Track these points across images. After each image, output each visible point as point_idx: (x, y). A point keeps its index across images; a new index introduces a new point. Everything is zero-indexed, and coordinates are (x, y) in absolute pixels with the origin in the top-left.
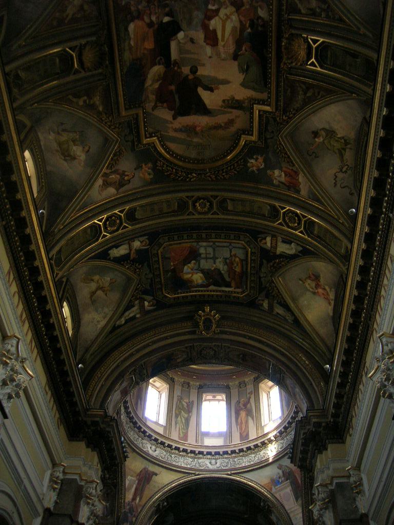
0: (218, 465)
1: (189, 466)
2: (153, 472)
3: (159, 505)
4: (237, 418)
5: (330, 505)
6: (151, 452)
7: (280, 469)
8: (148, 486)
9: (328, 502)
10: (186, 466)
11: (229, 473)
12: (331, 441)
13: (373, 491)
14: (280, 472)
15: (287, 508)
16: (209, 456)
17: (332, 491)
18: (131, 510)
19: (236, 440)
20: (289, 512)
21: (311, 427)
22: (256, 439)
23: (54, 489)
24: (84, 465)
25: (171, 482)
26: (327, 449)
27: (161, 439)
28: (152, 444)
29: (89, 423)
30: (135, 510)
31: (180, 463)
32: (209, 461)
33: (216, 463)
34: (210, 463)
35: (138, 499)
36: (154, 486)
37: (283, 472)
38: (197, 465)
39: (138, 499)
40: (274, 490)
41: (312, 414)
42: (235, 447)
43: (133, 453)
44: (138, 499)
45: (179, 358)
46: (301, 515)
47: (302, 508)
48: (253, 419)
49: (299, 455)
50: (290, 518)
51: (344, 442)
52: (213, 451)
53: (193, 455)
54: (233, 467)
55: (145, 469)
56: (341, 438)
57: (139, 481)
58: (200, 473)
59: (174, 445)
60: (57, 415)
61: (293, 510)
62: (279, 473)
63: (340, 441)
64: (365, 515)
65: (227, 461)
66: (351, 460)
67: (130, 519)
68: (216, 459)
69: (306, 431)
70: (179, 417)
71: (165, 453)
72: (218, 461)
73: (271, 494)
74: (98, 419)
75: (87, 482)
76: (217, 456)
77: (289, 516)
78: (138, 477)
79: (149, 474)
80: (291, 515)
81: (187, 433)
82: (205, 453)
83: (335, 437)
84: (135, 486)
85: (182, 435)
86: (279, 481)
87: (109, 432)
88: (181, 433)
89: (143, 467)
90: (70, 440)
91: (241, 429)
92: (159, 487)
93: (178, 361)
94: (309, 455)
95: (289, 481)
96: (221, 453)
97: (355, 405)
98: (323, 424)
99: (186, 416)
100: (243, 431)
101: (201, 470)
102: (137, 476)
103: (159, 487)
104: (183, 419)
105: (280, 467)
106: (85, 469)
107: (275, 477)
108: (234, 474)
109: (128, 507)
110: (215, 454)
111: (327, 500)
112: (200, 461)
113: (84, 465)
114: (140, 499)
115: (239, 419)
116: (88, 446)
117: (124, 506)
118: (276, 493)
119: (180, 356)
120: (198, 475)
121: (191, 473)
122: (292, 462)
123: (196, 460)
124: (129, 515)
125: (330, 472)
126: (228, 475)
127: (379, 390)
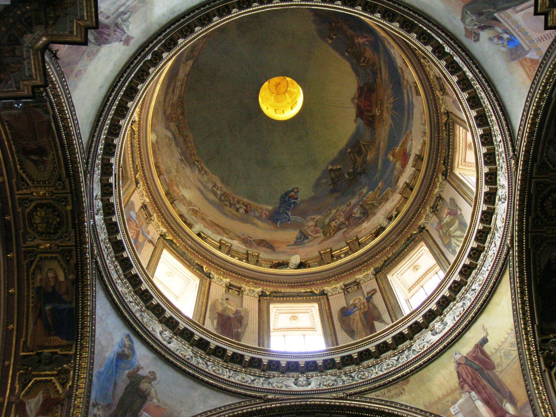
2: (477, 346)
7: (478, 35)
8: (497, 370)
14: (484, 35)
36: (507, 355)
37: (482, 28)
43: (408, 382)
45: (56, 278)
55: (459, 364)
57: (474, 388)
62: (491, 39)
78: (466, 387)
79: (476, 358)
84: (479, 404)
89: (452, 367)
92: (512, 345)
93: (62, 278)
95: (496, 15)
102: (462, 387)
107: (504, 49)
114: (513, 401)
118: (538, 50)
119: (51, 275)
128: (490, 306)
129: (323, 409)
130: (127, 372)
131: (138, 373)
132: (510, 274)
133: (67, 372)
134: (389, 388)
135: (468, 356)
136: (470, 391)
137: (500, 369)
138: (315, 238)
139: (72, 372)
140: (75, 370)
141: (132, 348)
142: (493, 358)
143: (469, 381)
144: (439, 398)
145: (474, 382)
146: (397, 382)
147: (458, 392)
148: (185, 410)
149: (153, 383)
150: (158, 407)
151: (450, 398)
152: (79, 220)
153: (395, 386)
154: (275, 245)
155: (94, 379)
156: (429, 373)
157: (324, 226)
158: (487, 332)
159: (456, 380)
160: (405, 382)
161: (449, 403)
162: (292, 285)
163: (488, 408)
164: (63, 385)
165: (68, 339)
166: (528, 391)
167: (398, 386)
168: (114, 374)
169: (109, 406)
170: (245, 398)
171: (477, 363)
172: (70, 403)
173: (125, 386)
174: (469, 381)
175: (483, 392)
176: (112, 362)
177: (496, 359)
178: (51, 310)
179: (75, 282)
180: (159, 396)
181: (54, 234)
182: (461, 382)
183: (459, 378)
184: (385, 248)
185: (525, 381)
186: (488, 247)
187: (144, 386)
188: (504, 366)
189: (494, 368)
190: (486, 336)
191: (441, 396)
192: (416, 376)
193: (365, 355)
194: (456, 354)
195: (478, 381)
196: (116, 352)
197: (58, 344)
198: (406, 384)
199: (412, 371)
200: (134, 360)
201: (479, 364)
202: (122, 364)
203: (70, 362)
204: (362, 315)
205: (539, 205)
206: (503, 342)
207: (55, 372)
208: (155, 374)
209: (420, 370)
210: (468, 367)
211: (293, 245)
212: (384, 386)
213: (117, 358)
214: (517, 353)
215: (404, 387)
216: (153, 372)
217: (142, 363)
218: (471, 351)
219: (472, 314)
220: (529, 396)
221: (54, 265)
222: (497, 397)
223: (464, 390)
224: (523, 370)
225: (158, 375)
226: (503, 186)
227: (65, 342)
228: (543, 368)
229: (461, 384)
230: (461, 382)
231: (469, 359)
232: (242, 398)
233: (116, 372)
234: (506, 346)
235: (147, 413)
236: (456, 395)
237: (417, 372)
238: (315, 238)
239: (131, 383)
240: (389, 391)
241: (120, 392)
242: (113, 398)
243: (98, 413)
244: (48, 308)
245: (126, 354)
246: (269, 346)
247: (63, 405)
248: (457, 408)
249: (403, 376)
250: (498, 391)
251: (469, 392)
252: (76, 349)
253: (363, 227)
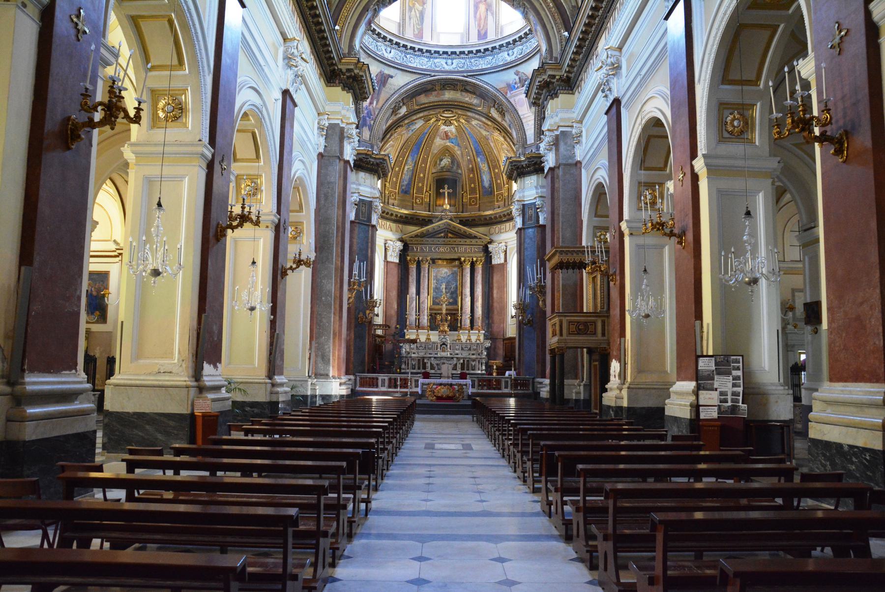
0: (454, 65)
1: (424, 67)
2: (389, 75)
3: (395, 106)
4: (475, 13)
5: (554, 148)
6: (386, 55)
7: (517, 75)
8: (384, 89)
9: (552, 145)
10: (421, 67)
11: (465, 74)
12: (562, 92)
13: (589, 145)
14: (517, 78)
15: (520, 113)
16: (445, 56)
17: (557, 136)
18: (369, 114)
19: (474, 39)
20: (521, 117)
21: (545, 77)
22: (495, 41)
23: (322, 136)
24: (343, 108)
25: (407, 84)
26: (558, 97)
27: (395, 40)
28: (386, 45)
29: (344, 70)
30: (373, 113)
31: (415, 64)
32: (445, 61)
33: (452, 63)
34: (446, 63)
36: (390, 88)
37: (520, 78)
38: (433, 65)
39: (375, 102)
40: (508, 95)
41: (549, 67)
42: (472, 47)
44: (375, 102)
46: (533, 122)
47: (535, 116)
48: (492, 14)
49: (533, 95)
50: (522, 124)
51: (573, 94)
52: (449, 50)
53: (428, 54)
54: (470, 69)
56: (572, 90)
58: (436, 74)
59: (409, 45)
60: (319, 71)
61: (525, 116)
62: (515, 79)
63: (571, 92)
64: (578, 164)
65: (463, 61)
66: (577, 112)
67: (368, 123)
68: (452, 59)
69: (541, 80)
70: (413, 10)
71: (400, 54)
72: (454, 61)
73: (506, 98)
74: (352, 67)
75: (347, 124)
76: (454, 56)
77: (521, 121)
80: (524, 121)
81: (422, 30)
82: (441, 53)
83: (567, 88)
85: (416, 32)
86: (514, 87)
87: (362, 76)
88: (416, 30)
89: (379, 71)
90: (327, 86)
91: (479, 25)
92: (394, 89)
94: (542, 97)
96: (458, 53)
97: (585, 72)
98: (557, 77)
99: (420, 8)
100: (481, 28)
101: (437, 71)
103: (394, 89)
104: (417, 12)
105: (517, 73)
106: (344, 112)
108: (470, 76)
109: (366, 112)
110: (450, 53)
111: (552, 143)
112: (436, 61)
113: (343, 108)
114: (377, 104)
115: (478, 14)
116: (343, 89)
117: (363, 111)
120: (434, 76)
121: (427, 75)
122: (526, 97)
123: (431, 60)
124: (367, 118)
125: (557, 119)
126: (464, 76)
127: (600, 85)
128: (405, 73)
142: (387, 84)
177: (388, 85)
192: (372, 60)
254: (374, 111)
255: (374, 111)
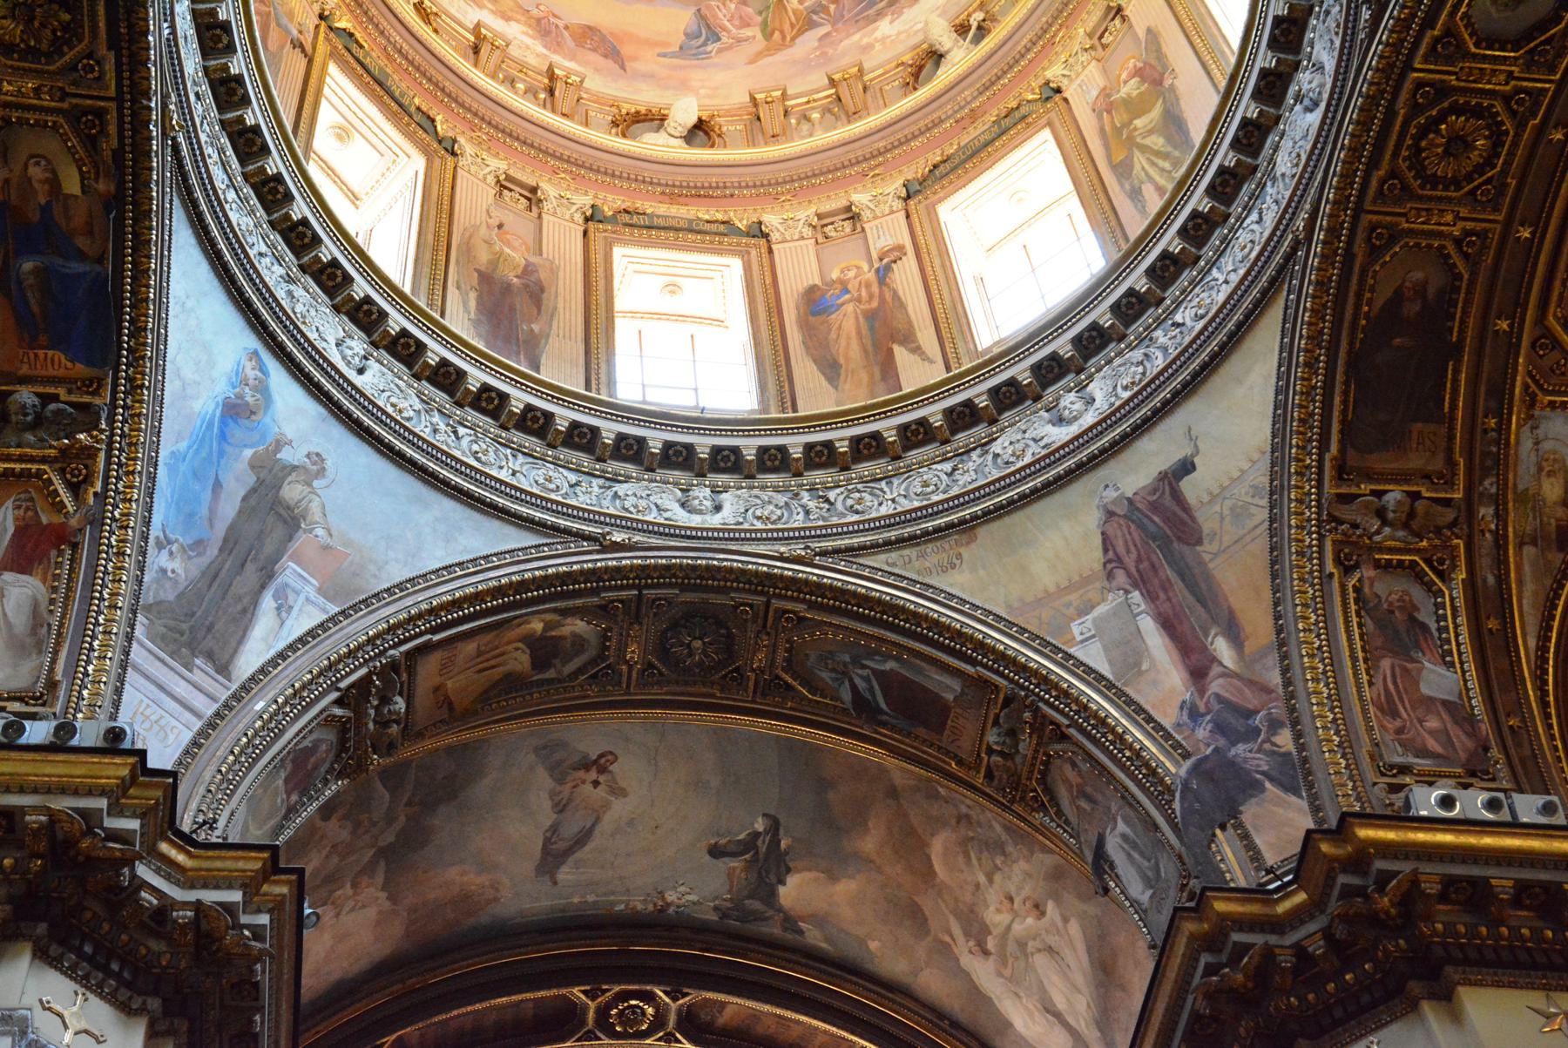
2: (1163, 476)
8: (1207, 548)
30: (1251, 700)
35: (1222, 649)
36: (1238, 513)
44: (1222, 649)
45: (54, 184)
55: (1110, 514)
57: (1140, 581)
78: (1121, 577)
79: (1155, 507)
84: (1148, 624)
89: (1092, 520)
93: (72, 184)
102: (1110, 576)
119: (36, 172)
129: (750, 583)
130: (248, 453)
131: (278, 456)
132: (1286, 308)
133: (89, 453)
134: (923, 547)
135: (1138, 498)
136: (1128, 587)
137: (1214, 547)
138: (739, 41)
139: (102, 455)
140: (110, 448)
141: (262, 389)
142: (1200, 516)
143: (1130, 561)
144: (1046, 591)
145: (1141, 567)
146: (949, 535)
147: (1098, 585)
148: (397, 561)
149: (316, 483)
150: (327, 548)
151: (1073, 597)
152: (130, 26)
153: (938, 544)
154: (626, 50)
155: (162, 473)
156: (1029, 524)
157: (768, 7)
158: (1196, 446)
159: (1098, 554)
160: (964, 538)
161: (1072, 611)
162: (674, 194)
163: (1167, 640)
164: (76, 489)
165: (89, 363)
166: (1277, 617)
167: (947, 546)
168: (215, 458)
169: (199, 545)
170: (554, 536)
171: (1156, 519)
172: (96, 541)
173: (242, 493)
174: (1130, 561)
175: (1162, 595)
176: (210, 424)
177: (1207, 520)
178: (36, 272)
179: (114, 202)
180: (331, 518)
181: (50, 57)
182: (1110, 561)
183: (1106, 551)
184: (942, 121)
185: (1276, 590)
186: (1241, 219)
187: (292, 491)
188: (1227, 540)
189: (1199, 542)
190: (1193, 456)
191: (1052, 589)
192: (995, 527)
193: (869, 446)
194: (1107, 486)
195: (1153, 566)
196: (220, 399)
197: (61, 372)
198: (968, 543)
199: (986, 513)
200: (267, 420)
201: (1162, 524)
202: (237, 432)
203: (96, 427)
204: (861, 319)
205: (1409, 142)
206: (1233, 480)
207: (53, 452)
208: (323, 460)
209: (1008, 513)
210: (1133, 527)
211: (673, 55)
212: (911, 540)
213: (223, 415)
214: (1265, 514)
215: (963, 550)
216: (318, 455)
217: (289, 431)
218: (1144, 488)
219: (1165, 394)
220: (1279, 630)
221: (49, 145)
222: (1196, 615)
223: (1114, 584)
224: (1273, 563)
225: (329, 464)
226: (1320, 68)
227: (81, 369)
228: (1330, 567)
229: (1109, 566)
230: (1110, 561)
231: (1139, 505)
232: (547, 535)
233: (221, 453)
234: (1242, 492)
235: (299, 564)
236: (1093, 595)
237: (999, 517)
238: (739, 41)
239: (260, 482)
240: (922, 556)
241: (229, 508)
242: (211, 526)
243: (169, 566)
244: (28, 266)
245: (247, 404)
246: (611, 383)
247: (75, 547)
248: (1089, 624)
249: (962, 522)
250: (1202, 601)
251: (1127, 592)
252: (114, 392)
253: (878, 34)
254: (1251, 683)
255: (1251, 683)
